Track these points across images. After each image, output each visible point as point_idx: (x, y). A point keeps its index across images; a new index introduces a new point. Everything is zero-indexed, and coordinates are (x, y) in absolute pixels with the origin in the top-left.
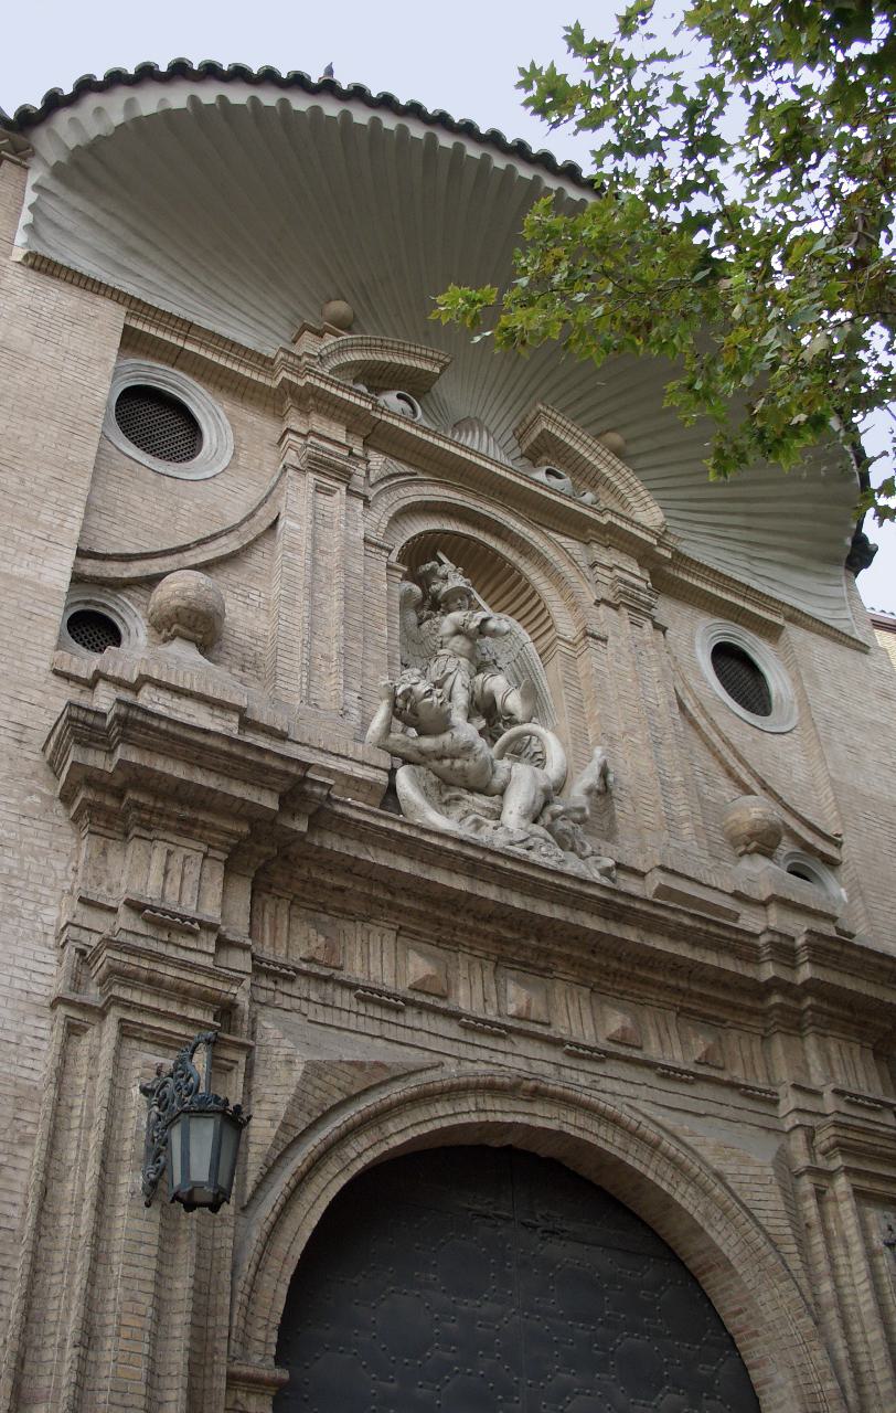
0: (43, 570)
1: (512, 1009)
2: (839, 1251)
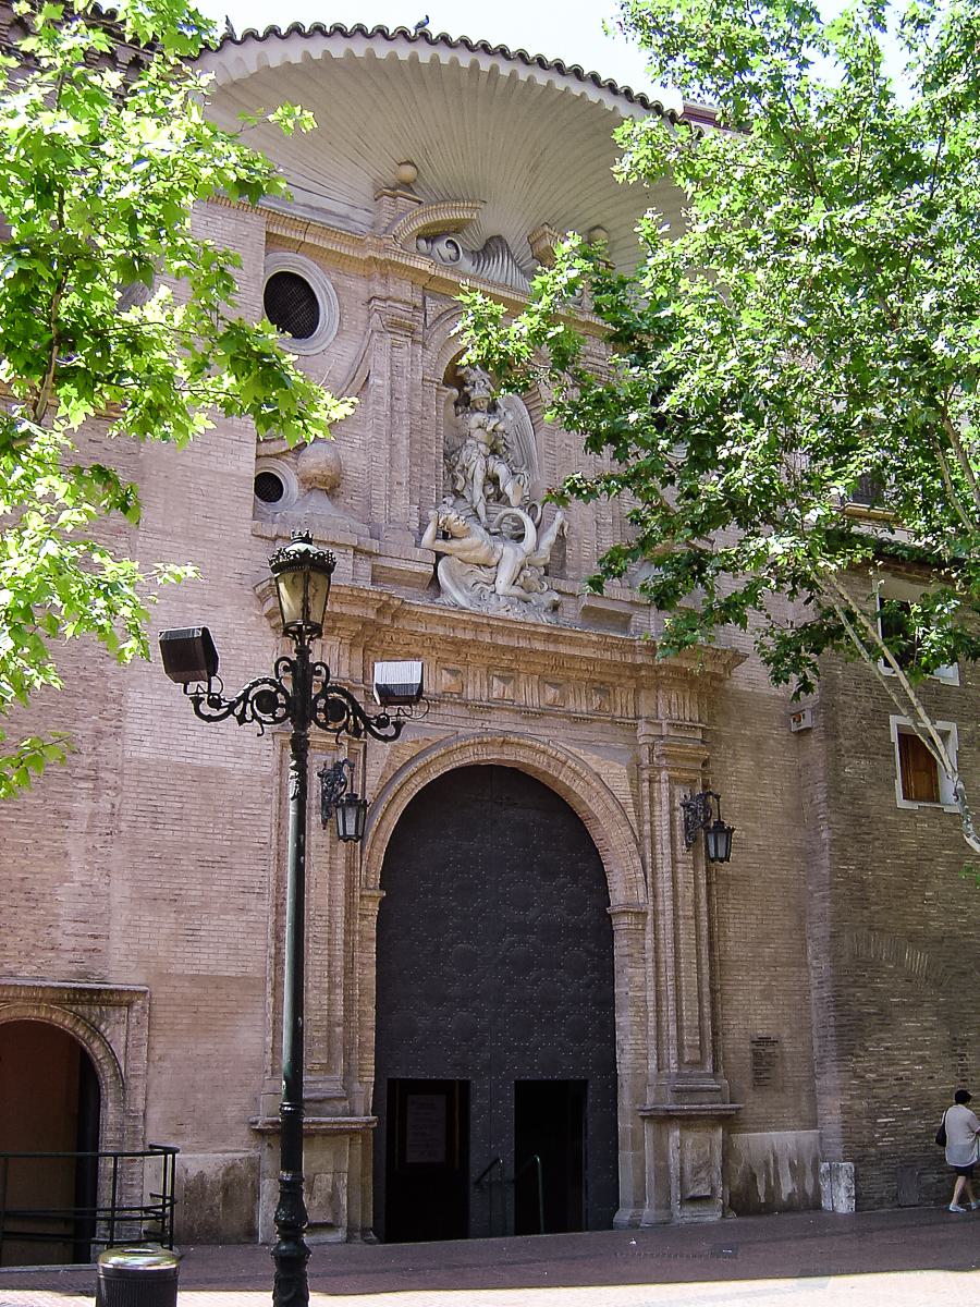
0: (240, 464)
1: (495, 695)
2: (657, 808)
